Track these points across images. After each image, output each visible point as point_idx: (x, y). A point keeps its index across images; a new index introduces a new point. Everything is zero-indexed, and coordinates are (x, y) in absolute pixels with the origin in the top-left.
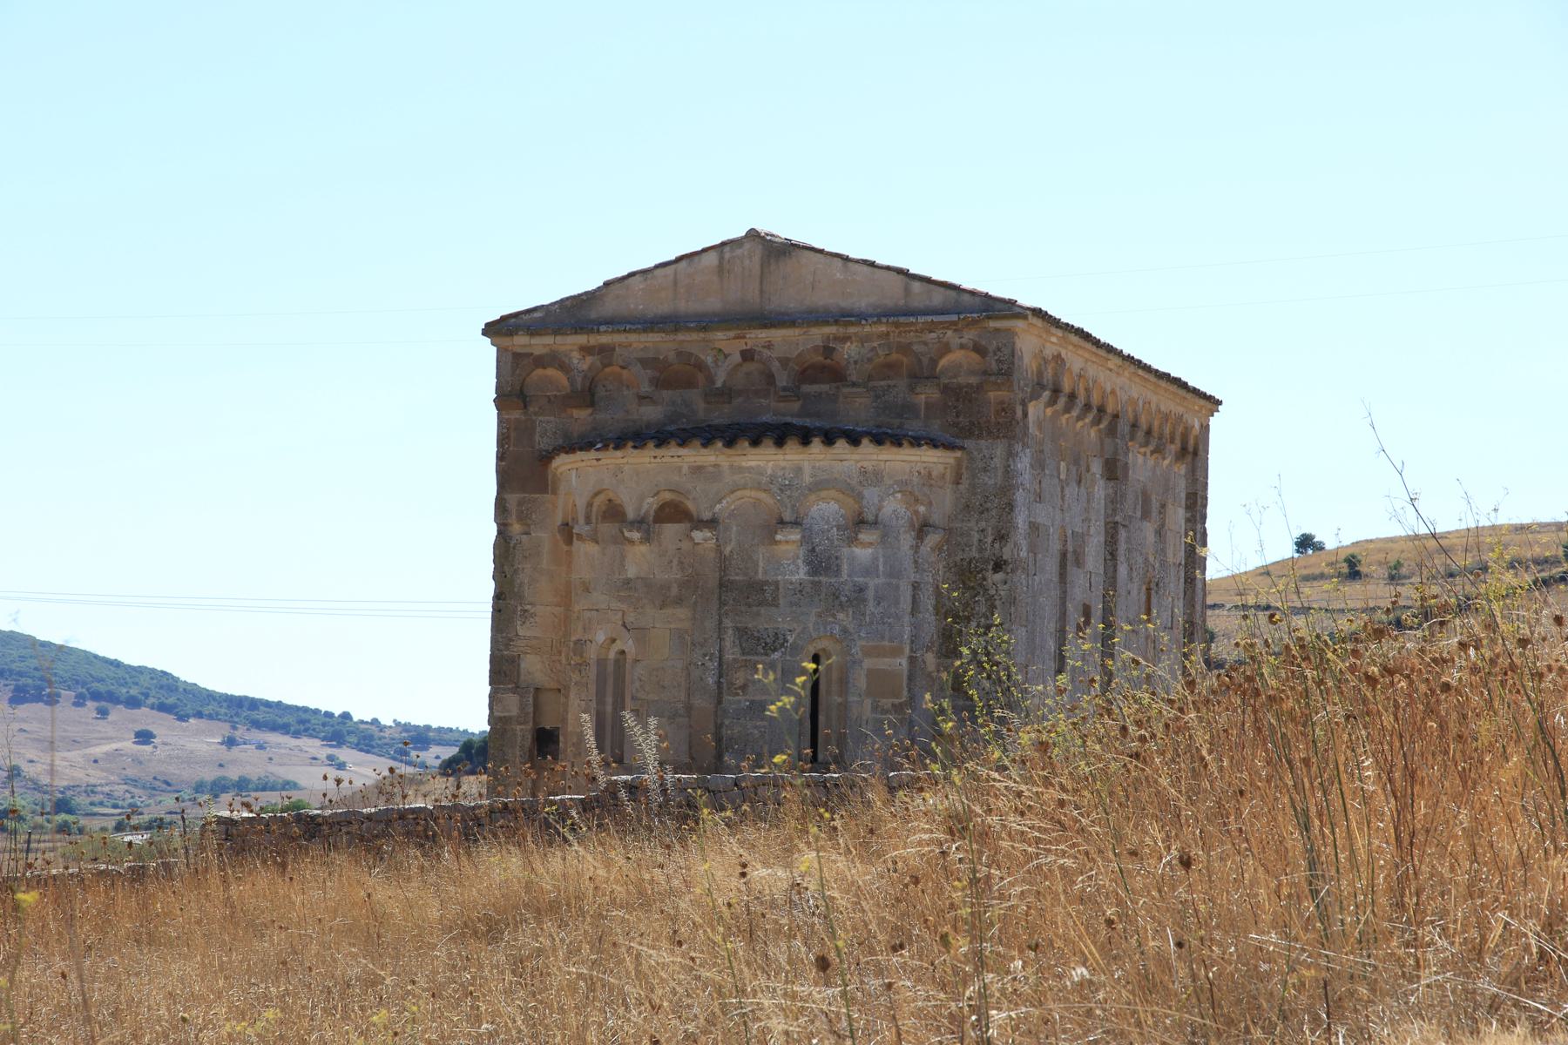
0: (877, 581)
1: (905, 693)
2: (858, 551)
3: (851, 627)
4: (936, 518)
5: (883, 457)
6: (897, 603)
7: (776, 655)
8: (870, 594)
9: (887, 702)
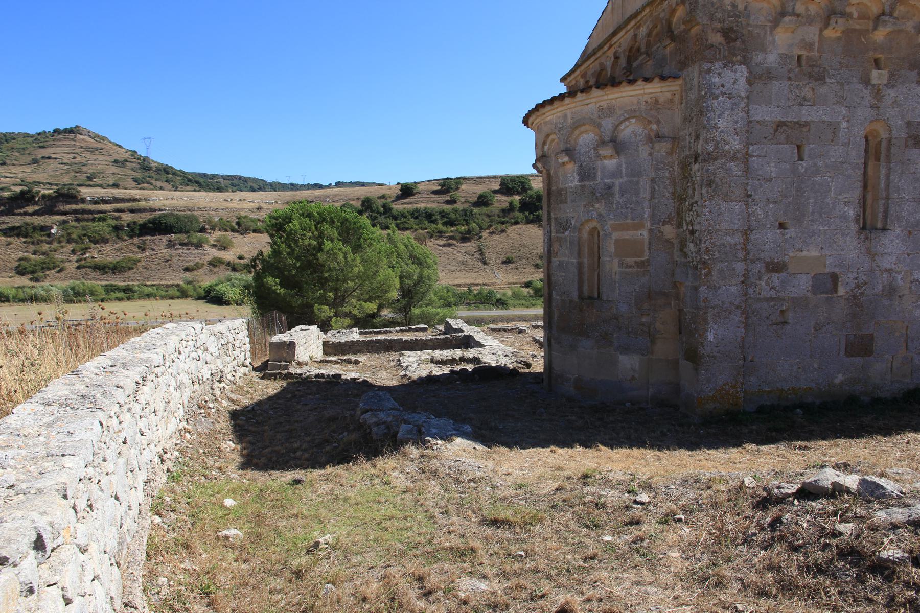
0: (621, 180)
1: (647, 253)
2: (606, 162)
3: (604, 213)
4: (666, 130)
7: (567, 233)
8: (617, 189)
9: (631, 261)
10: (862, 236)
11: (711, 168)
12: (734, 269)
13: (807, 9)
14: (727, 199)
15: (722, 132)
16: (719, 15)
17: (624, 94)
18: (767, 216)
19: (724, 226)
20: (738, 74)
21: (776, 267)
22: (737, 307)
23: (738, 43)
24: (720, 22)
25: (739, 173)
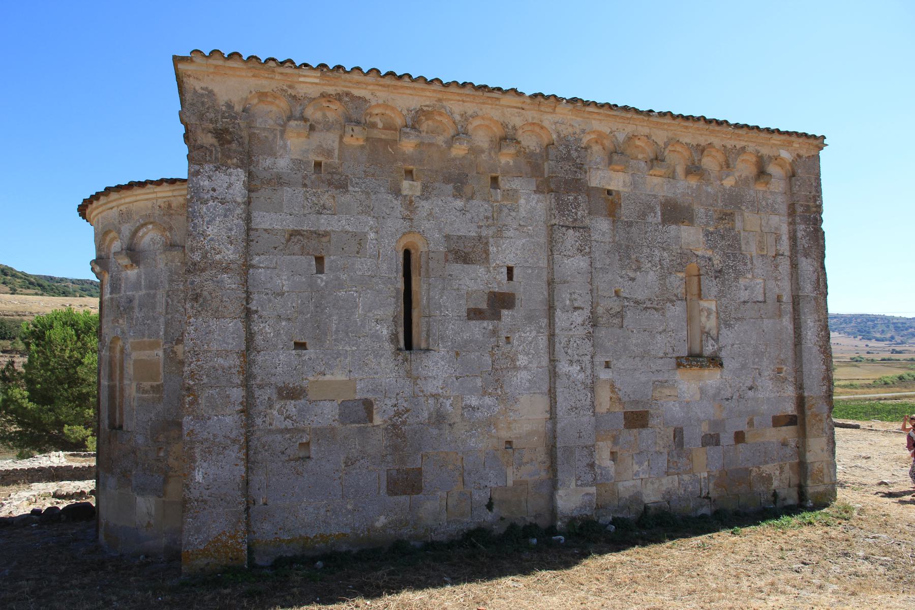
0: (141, 293)
5: (127, 200)
6: (154, 308)
10: (400, 358)
11: (197, 280)
12: (228, 396)
13: (324, 116)
14: (217, 315)
15: (212, 240)
16: (211, 115)
17: (139, 198)
18: (278, 334)
19: (214, 347)
20: (233, 178)
21: (291, 393)
22: (234, 441)
23: (234, 146)
24: (211, 121)
25: (233, 286)
